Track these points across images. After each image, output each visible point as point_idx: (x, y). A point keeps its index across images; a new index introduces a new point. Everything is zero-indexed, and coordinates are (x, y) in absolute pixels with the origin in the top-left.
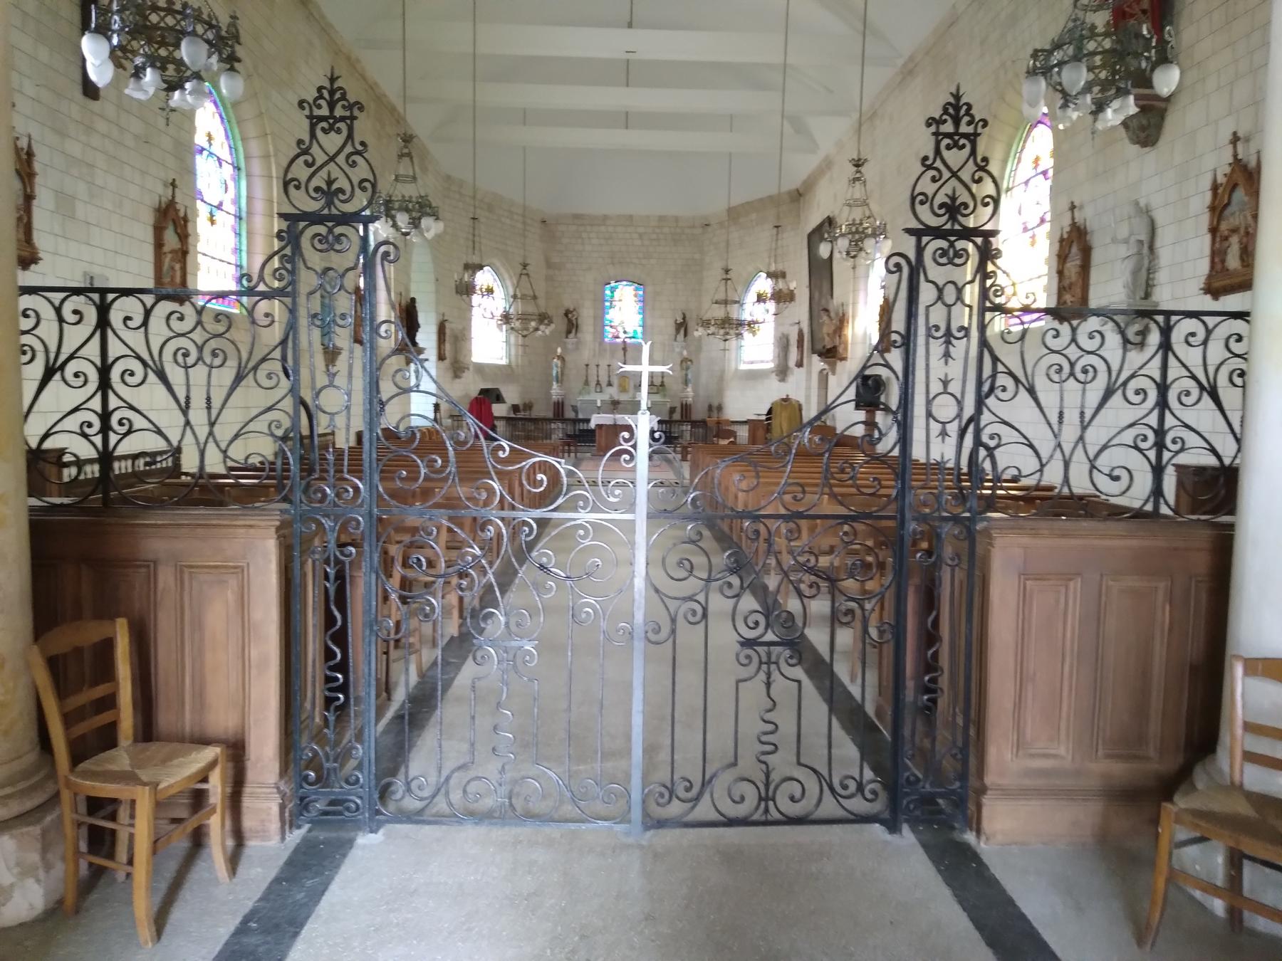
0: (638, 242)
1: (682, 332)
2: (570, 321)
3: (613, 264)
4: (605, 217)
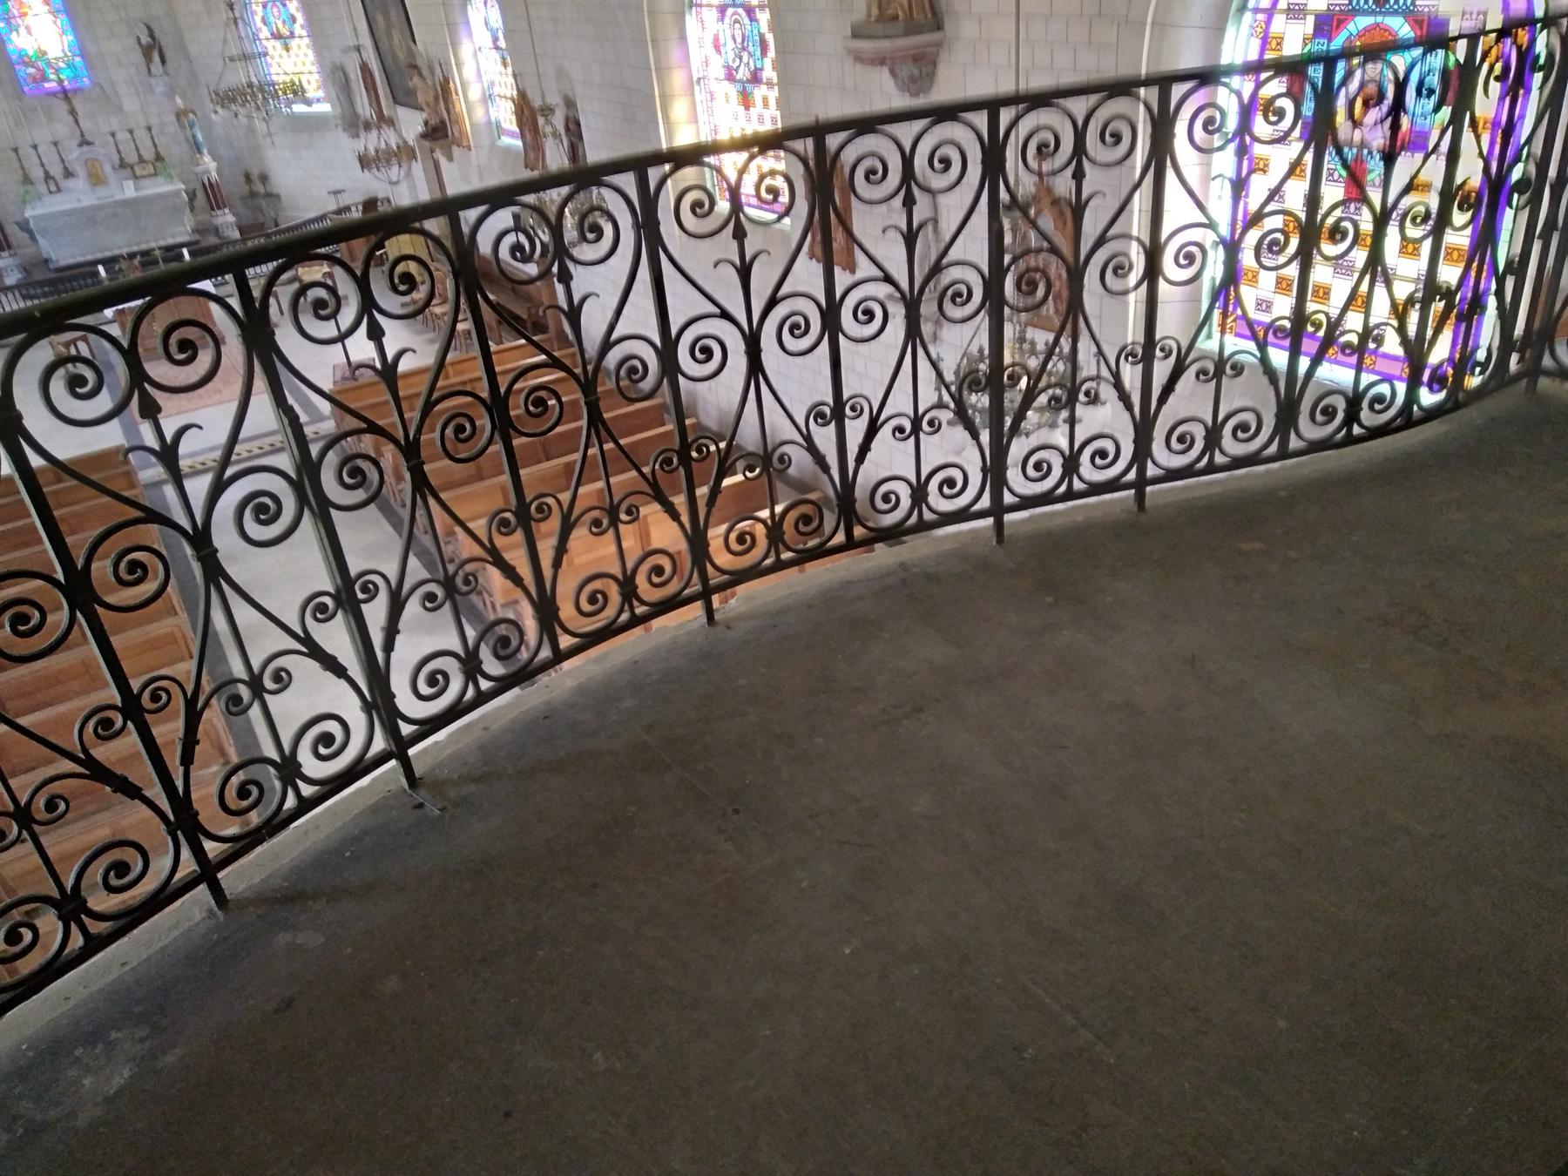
1: (156, 58)
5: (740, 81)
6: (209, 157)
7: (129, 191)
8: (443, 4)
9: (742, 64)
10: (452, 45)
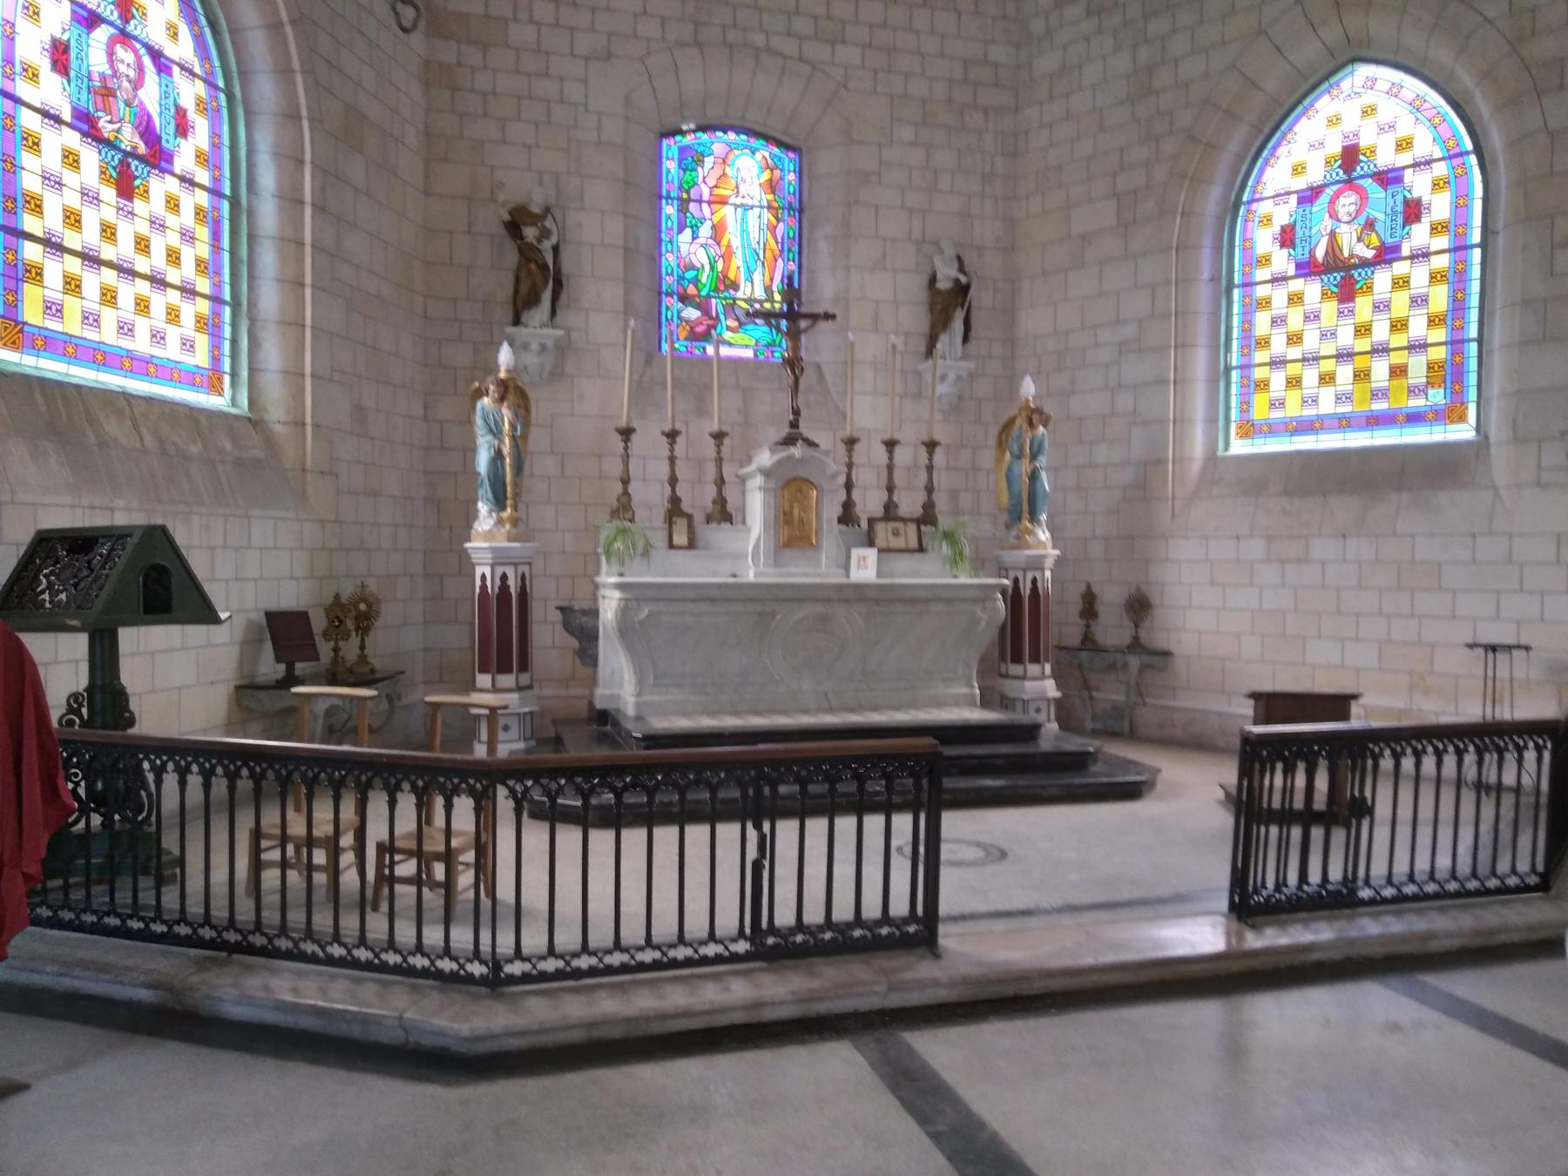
2: (528, 253)
7: (865, 567)
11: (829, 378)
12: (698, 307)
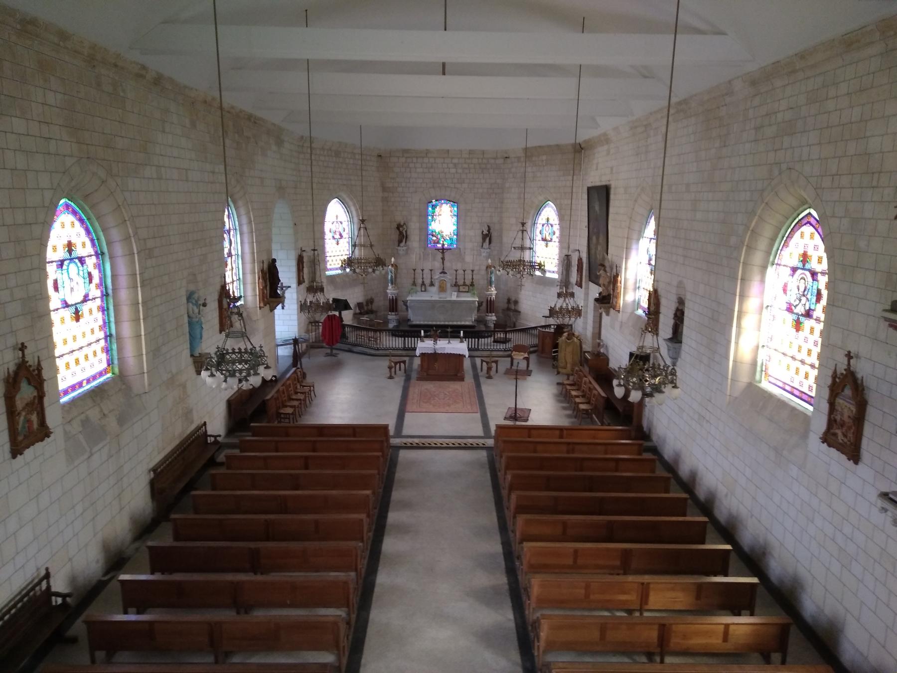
0: (453, 171)
2: (401, 233)
3: (433, 187)
4: (428, 152)
5: (797, 314)
6: (494, 289)
7: (454, 297)
8: (627, 238)
9: (800, 304)
10: (626, 258)
11: (461, 250)
12: (436, 237)
